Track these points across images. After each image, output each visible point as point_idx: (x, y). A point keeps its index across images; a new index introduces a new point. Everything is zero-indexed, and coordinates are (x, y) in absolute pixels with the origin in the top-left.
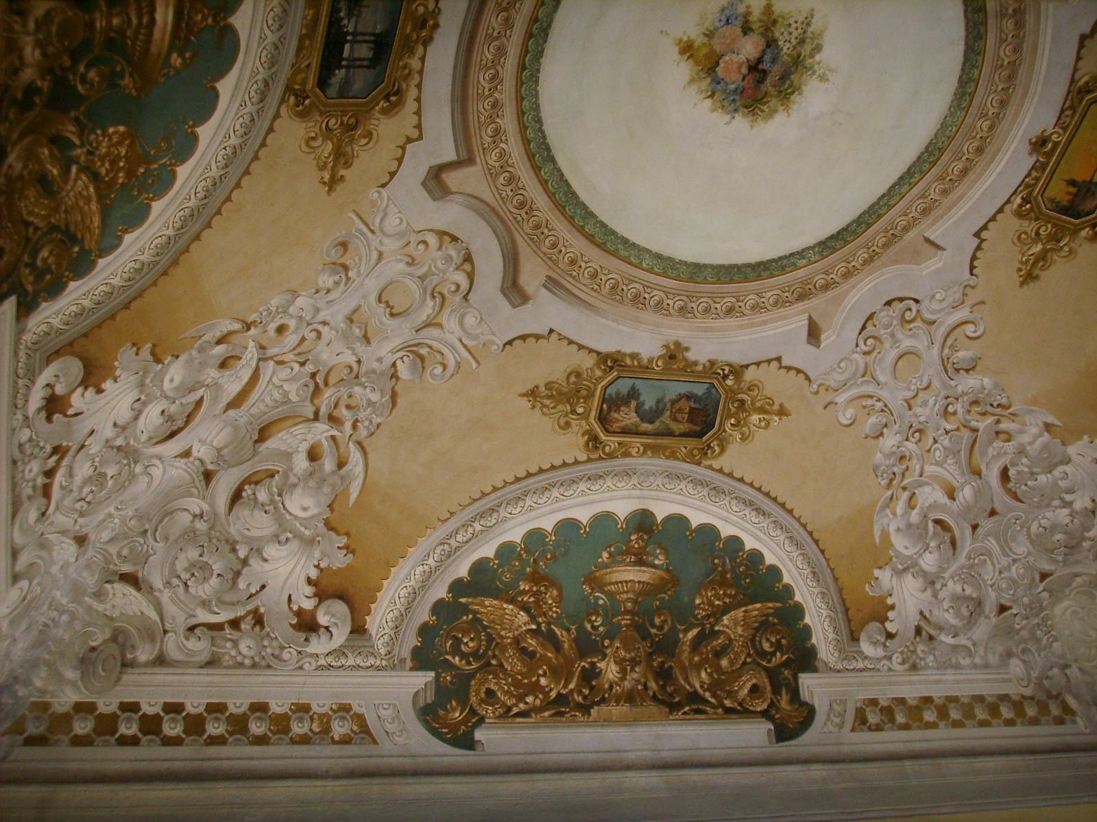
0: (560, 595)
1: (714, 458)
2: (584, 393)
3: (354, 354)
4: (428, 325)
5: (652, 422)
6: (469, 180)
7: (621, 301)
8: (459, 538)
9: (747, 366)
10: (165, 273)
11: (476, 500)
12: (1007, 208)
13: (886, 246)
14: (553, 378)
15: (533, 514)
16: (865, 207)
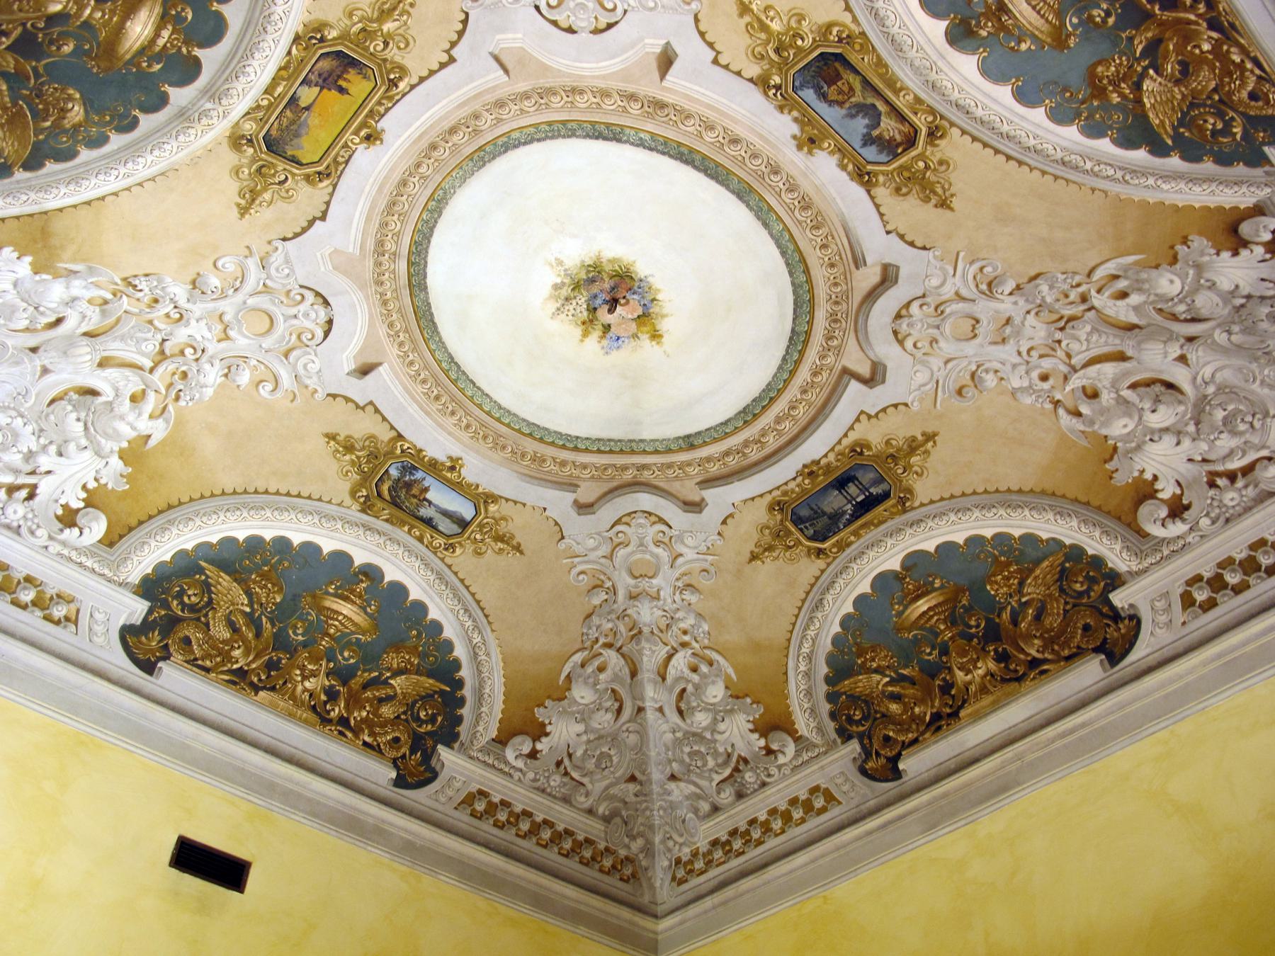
0: (1099, 63)
1: (844, 25)
2: (906, 174)
3: (1025, 318)
4: (964, 299)
5: (874, 106)
6: (855, 360)
7: (819, 213)
8: (1111, 172)
9: (751, 80)
10: (1053, 494)
11: (1067, 181)
12: (415, 80)
13: (551, 92)
14: (919, 202)
15: (1038, 132)
16: (560, 142)
